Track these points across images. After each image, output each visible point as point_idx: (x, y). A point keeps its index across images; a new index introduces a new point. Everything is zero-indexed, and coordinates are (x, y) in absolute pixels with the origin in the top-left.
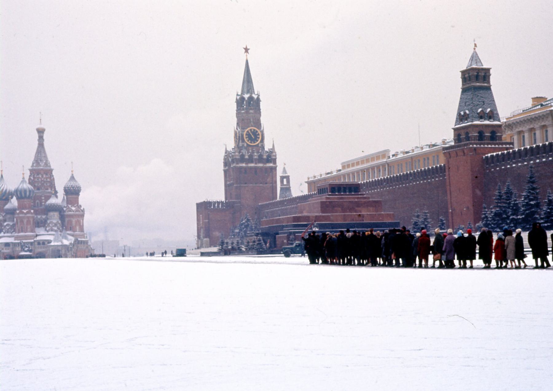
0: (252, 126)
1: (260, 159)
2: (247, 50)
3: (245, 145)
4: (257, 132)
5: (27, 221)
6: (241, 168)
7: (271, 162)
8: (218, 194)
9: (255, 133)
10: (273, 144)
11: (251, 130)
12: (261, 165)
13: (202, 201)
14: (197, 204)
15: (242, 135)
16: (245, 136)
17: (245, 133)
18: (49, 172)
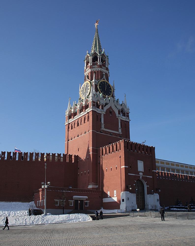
0: (104, 79)
4: (109, 86)
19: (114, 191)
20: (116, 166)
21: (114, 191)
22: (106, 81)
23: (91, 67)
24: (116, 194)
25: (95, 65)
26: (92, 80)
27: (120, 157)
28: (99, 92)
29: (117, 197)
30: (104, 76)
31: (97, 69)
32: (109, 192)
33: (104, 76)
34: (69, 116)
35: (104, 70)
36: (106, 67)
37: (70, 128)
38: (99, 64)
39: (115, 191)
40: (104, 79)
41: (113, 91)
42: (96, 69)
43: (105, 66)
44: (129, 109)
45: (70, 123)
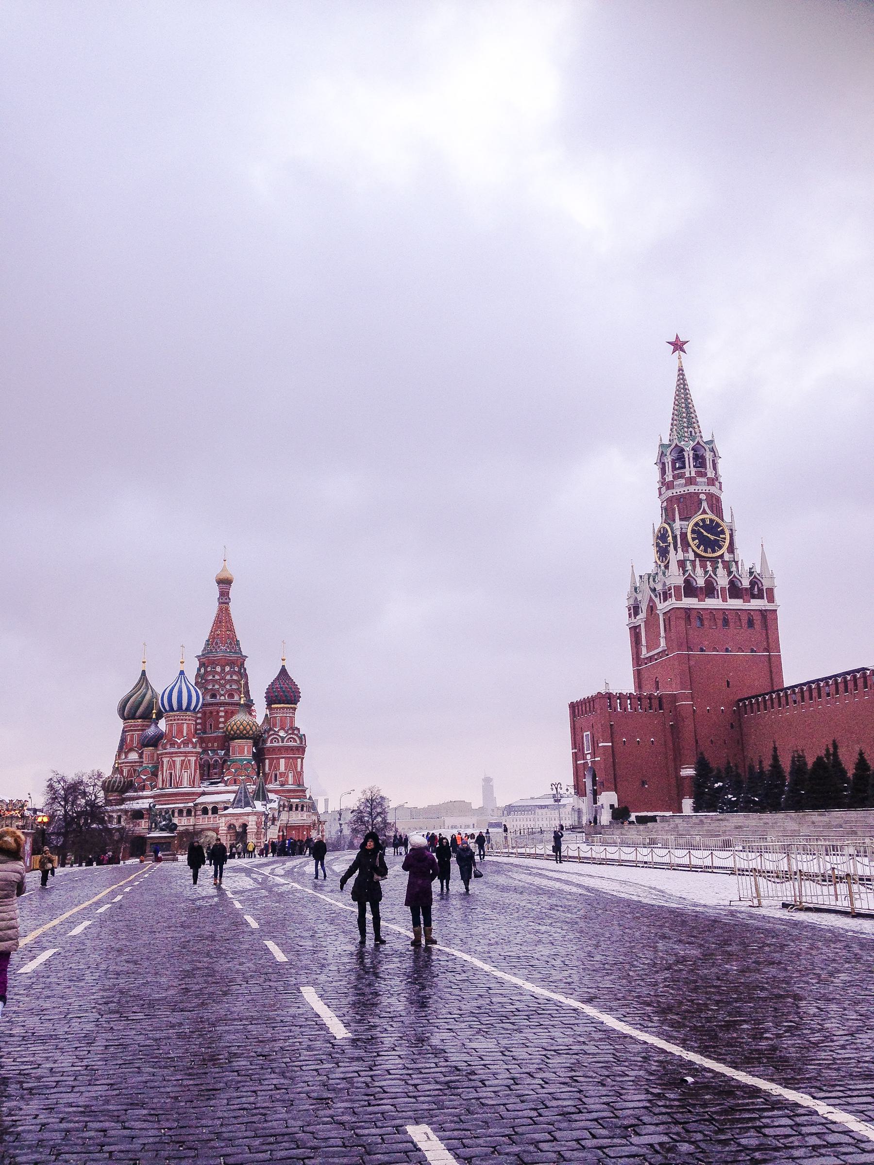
0: (704, 512)
1: (735, 591)
2: (678, 346)
3: (691, 556)
4: (718, 525)
5: (183, 761)
6: (688, 611)
7: (763, 598)
8: (624, 683)
9: (714, 528)
10: (763, 553)
11: (703, 520)
12: (736, 604)
13: (590, 692)
14: (572, 706)
15: (684, 535)
16: (689, 536)
17: (689, 530)
18: (238, 663)
22: (710, 516)
23: (669, 486)
26: (674, 521)
28: (693, 551)
30: (705, 505)
31: (686, 489)
33: (705, 505)
35: (701, 487)
38: (687, 475)
40: (704, 512)
41: (731, 536)
42: (682, 490)
43: (706, 474)
44: (772, 578)
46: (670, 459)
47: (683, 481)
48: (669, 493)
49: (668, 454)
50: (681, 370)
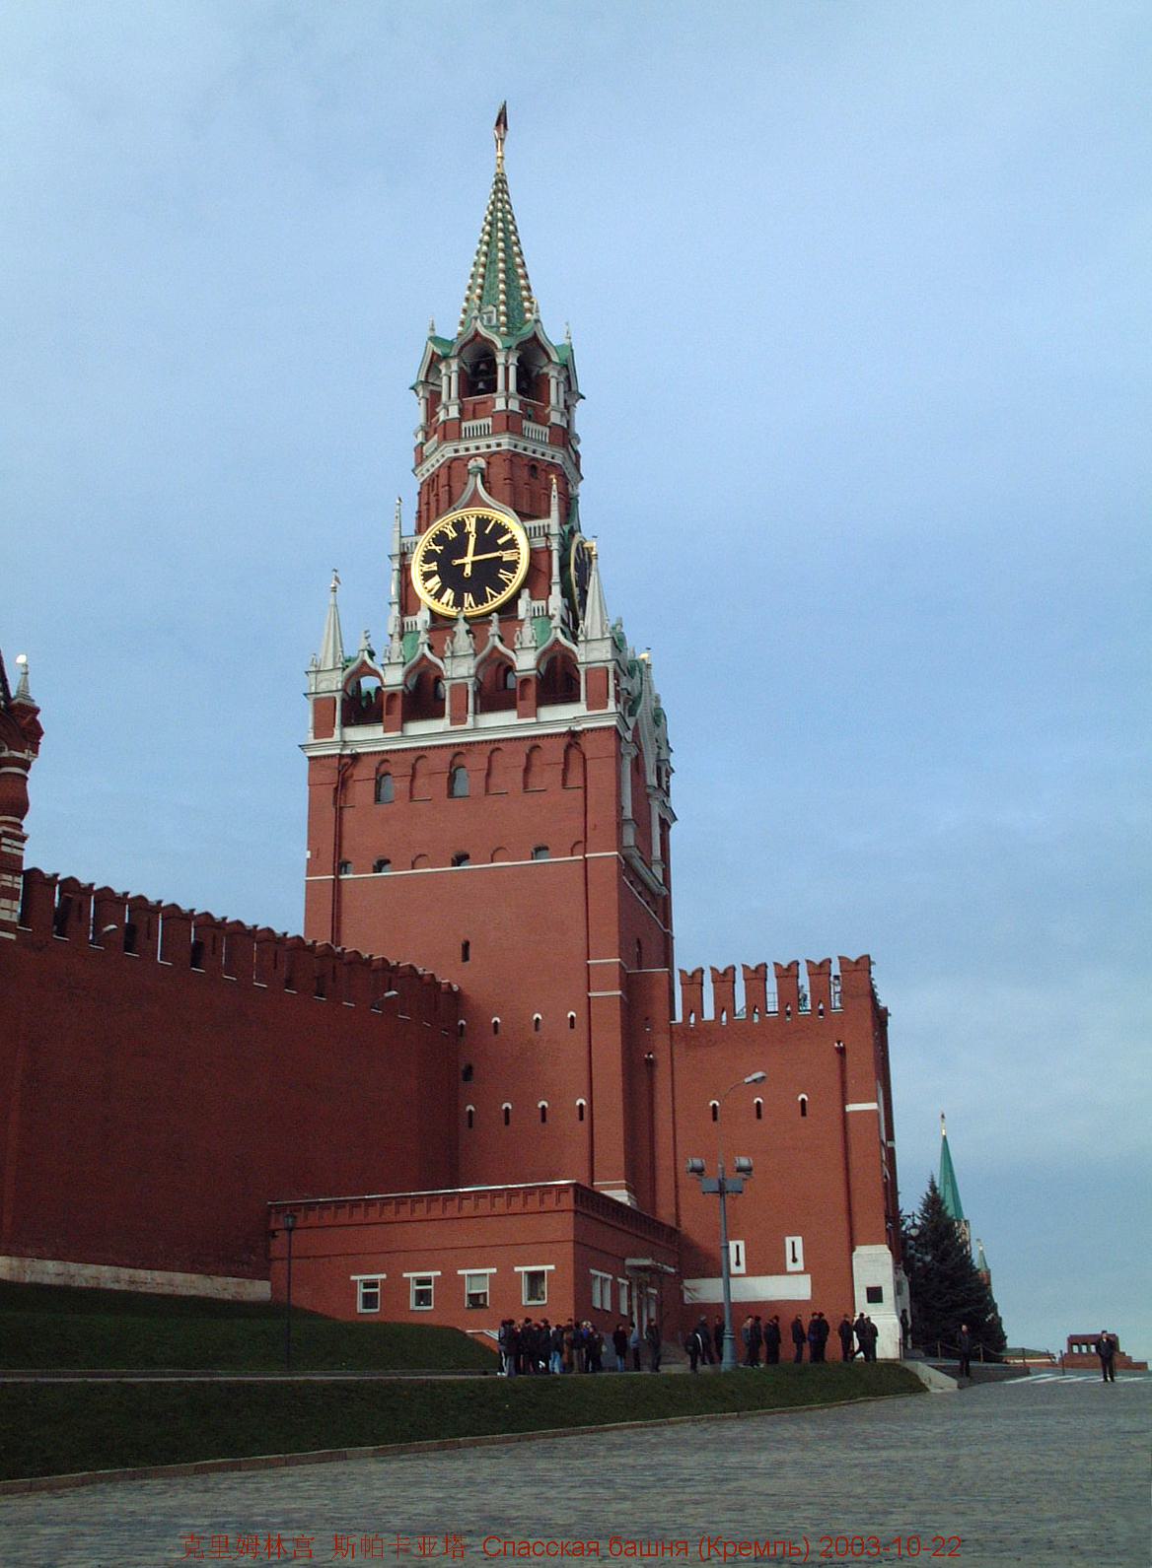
19: (788, 1240)
20: (804, 1096)
21: (788, 1240)
24: (799, 1254)
25: (529, 418)
27: (842, 1051)
29: (807, 1279)
31: (549, 452)
32: (741, 1244)
34: (343, 701)
36: (576, 453)
37: (361, 790)
38: (555, 418)
39: (794, 1244)
42: (540, 450)
45: (356, 758)
46: (513, 360)
47: (547, 430)
48: (505, 442)
49: (514, 347)
50: (501, 180)
